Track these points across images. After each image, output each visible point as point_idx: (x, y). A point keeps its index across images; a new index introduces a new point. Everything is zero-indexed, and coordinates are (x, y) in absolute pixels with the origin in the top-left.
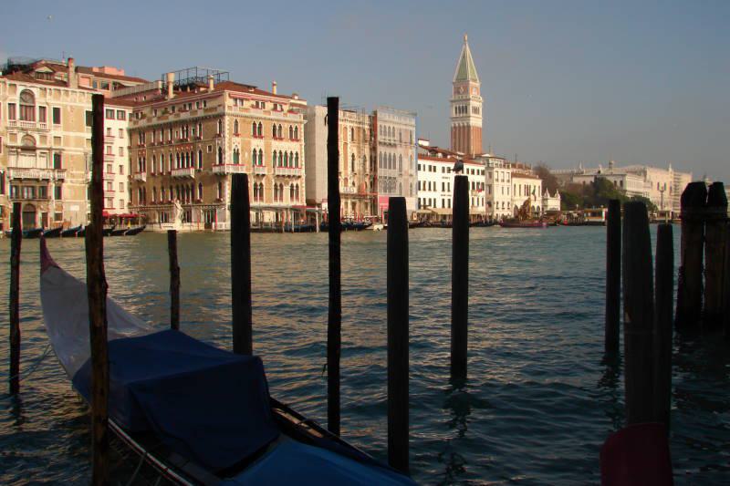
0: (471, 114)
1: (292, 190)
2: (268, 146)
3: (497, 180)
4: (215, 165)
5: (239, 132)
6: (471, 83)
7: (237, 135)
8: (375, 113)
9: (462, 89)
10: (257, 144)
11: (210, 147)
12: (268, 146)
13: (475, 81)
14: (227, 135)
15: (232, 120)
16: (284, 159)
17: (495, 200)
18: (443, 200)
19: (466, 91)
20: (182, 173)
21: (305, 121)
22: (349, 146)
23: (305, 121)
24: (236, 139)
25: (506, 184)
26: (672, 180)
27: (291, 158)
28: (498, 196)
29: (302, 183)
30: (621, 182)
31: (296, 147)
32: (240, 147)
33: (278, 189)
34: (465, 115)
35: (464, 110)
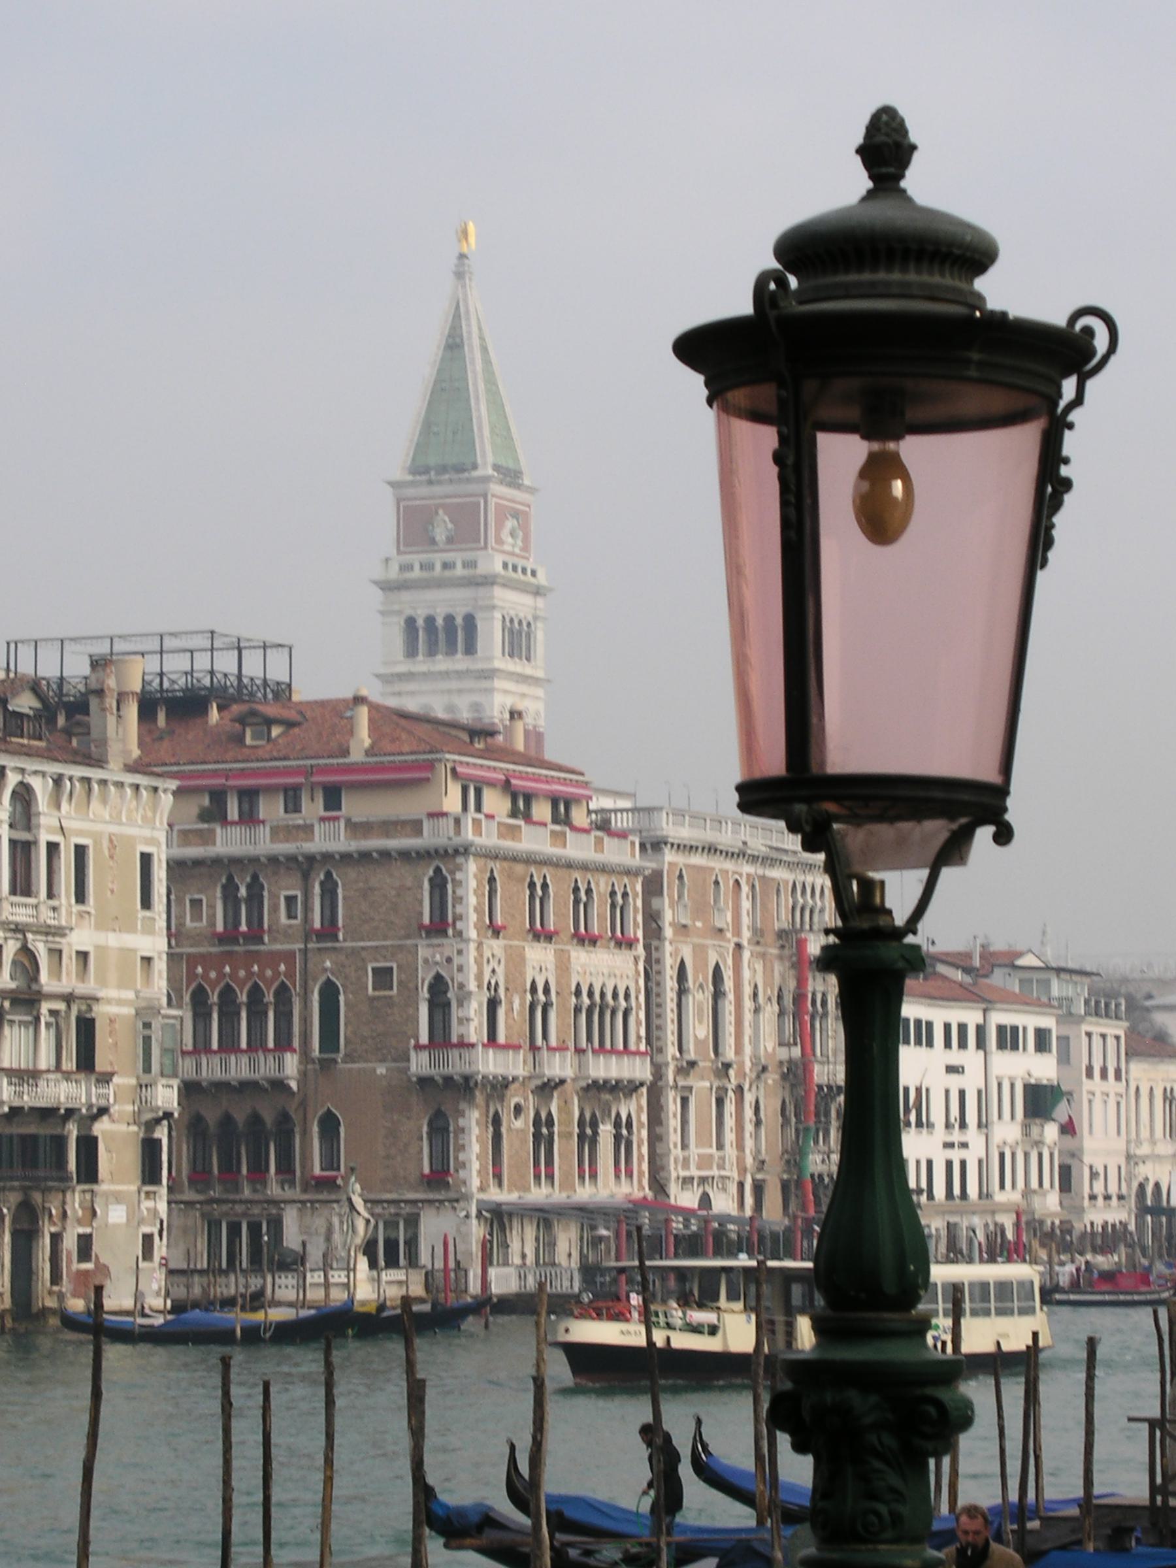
1: (618, 1137)
2: (563, 966)
3: (1090, 1075)
4: (418, 1047)
5: (499, 920)
6: (496, 488)
7: (496, 932)
9: (442, 529)
10: (539, 959)
11: (383, 976)
12: (563, 966)
15: (481, 870)
17: (1087, 1159)
18: (949, 1164)
20: (239, 1068)
22: (746, 955)
24: (496, 946)
27: (613, 1013)
28: (1100, 1146)
29: (640, 1108)
31: (608, 968)
34: (460, 662)
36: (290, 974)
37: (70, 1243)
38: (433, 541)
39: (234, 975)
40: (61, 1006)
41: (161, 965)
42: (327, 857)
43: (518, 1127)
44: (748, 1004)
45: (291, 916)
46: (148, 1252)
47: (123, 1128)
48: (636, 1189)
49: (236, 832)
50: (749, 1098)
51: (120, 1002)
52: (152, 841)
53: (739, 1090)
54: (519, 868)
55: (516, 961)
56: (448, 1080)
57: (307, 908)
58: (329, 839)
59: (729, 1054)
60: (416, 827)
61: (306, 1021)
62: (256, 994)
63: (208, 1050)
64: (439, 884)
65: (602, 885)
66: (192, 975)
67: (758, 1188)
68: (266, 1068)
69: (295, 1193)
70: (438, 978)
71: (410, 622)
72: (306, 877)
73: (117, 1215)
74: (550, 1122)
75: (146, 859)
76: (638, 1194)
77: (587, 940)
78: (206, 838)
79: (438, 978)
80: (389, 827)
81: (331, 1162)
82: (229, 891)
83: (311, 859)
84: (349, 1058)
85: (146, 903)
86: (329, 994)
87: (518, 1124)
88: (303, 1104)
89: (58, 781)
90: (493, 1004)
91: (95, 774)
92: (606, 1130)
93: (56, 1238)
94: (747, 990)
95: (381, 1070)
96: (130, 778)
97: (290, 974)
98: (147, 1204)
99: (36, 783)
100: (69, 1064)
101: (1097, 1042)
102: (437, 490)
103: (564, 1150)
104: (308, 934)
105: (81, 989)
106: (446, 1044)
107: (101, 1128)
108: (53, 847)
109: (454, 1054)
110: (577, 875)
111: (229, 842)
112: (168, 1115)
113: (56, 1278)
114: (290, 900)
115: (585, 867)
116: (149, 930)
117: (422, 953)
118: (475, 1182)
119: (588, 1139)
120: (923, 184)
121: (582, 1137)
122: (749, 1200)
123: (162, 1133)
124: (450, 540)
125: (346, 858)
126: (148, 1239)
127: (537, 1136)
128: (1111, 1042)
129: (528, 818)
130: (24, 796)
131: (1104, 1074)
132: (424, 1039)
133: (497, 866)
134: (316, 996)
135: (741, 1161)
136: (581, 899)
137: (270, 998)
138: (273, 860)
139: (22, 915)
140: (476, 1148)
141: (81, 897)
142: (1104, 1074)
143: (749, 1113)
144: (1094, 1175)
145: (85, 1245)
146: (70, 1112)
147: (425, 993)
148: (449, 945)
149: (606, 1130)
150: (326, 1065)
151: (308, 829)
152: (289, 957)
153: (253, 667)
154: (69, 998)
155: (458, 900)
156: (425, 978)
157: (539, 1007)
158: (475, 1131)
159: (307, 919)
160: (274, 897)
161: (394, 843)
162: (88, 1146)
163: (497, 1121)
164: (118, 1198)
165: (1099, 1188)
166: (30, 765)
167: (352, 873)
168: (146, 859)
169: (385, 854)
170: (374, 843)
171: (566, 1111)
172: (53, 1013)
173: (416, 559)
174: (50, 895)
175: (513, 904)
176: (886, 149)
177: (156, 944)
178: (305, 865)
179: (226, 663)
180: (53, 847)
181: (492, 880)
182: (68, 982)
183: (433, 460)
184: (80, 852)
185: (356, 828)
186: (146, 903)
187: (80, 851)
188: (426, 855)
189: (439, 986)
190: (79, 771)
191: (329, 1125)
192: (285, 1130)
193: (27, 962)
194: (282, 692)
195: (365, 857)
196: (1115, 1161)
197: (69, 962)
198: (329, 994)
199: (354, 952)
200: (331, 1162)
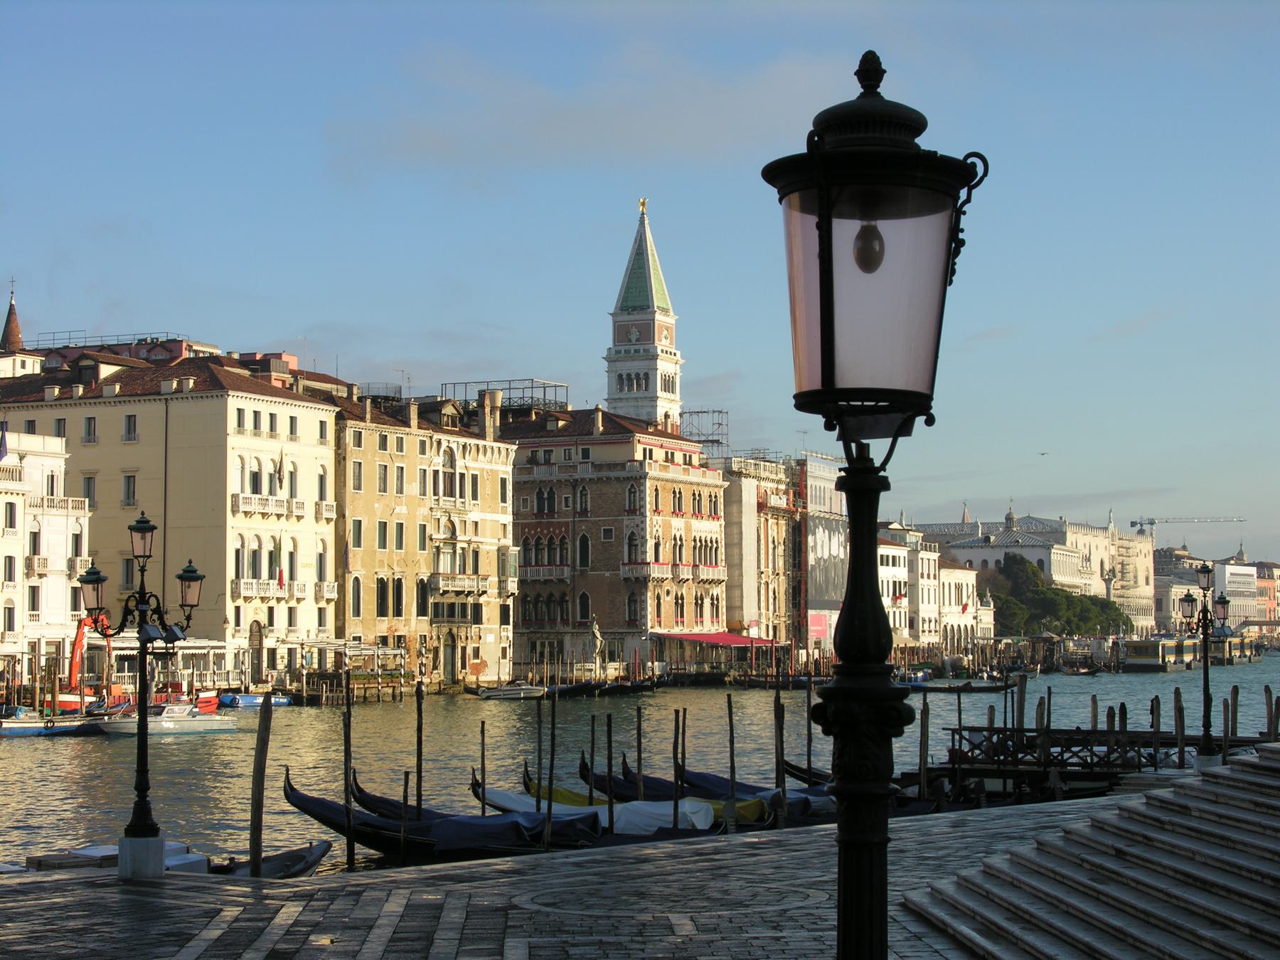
0: (660, 393)
1: (712, 604)
2: (688, 528)
6: (659, 317)
8: (802, 463)
9: (634, 335)
10: (678, 524)
11: (608, 533)
13: (665, 311)
14: (648, 514)
16: (704, 550)
17: (921, 615)
19: (647, 332)
20: (543, 573)
21: (727, 484)
23: (727, 484)
25: (932, 582)
26: (1113, 551)
28: (927, 610)
30: (1041, 562)
31: (710, 529)
32: (660, 533)
33: (699, 604)
34: (642, 394)
35: (645, 379)
36: (567, 531)
37: (469, 651)
38: (630, 340)
39: (542, 532)
40: (465, 545)
41: (510, 528)
42: (583, 480)
43: (668, 601)
44: (771, 546)
45: (567, 506)
46: (504, 656)
47: (492, 600)
48: (722, 628)
49: (543, 468)
50: (771, 587)
51: (491, 544)
52: (507, 473)
53: (767, 584)
54: (669, 485)
55: (667, 526)
56: (637, 579)
57: (575, 502)
59: (763, 568)
60: (623, 466)
62: (551, 541)
63: (530, 565)
65: (705, 493)
66: (523, 532)
67: (775, 628)
68: (555, 574)
69: (569, 629)
71: (620, 376)
72: (574, 488)
73: (490, 638)
74: (682, 598)
75: (503, 481)
76: (721, 630)
78: (530, 471)
79: (633, 533)
80: (612, 466)
82: (540, 494)
84: (593, 569)
85: (504, 500)
86: (584, 541)
87: (668, 599)
88: (573, 589)
89: (464, 447)
90: (657, 546)
91: (481, 443)
92: (707, 602)
93: (464, 649)
94: (770, 540)
95: (607, 574)
96: (496, 445)
97: (567, 531)
98: (504, 634)
99: (454, 446)
100: (469, 570)
101: (926, 562)
102: (632, 317)
103: (689, 608)
104: (575, 513)
105: (474, 539)
106: (636, 563)
107: (482, 600)
108: (462, 476)
110: (695, 487)
111: (539, 473)
112: (513, 594)
113: (464, 666)
114: (566, 499)
115: (698, 484)
116: (504, 511)
117: (626, 522)
118: (649, 625)
119: (699, 604)
120: (889, 90)
121: (696, 604)
122: (771, 633)
123: (510, 602)
124: (638, 340)
126: (504, 650)
127: (677, 603)
128: (932, 563)
129: (672, 461)
130: (450, 454)
131: (929, 577)
132: (626, 561)
133: (659, 484)
134: (578, 543)
135: (767, 616)
136: (697, 498)
137: (557, 542)
138: (559, 481)
139: (449, 506)
140: (649, 609)
141: (475, 497)
142: (929, 577)
143: (771, 594)
144: (924, 620)
145: (476, 652)
146: (470, 593)
147: (626, 541)
148: (637, 519)
149: (707, 602)
152: (567, 523)
153: (550, 396)
157: (678, 546)
158: (649, 601)
159: (574, 508)
160: (560, 497)
161: (613, 474)
162: (477, 608)
163: (659, 598)
164: (491, 631)
165: (926, 626)
166: (452, 438)
168: (503, 481)
170: (604, 474)
171: (689, 592)
172: (463, 549)
173: (623, 349)
174: (461, 497)
175: (667, 502)
176: (870, 70)
177: (508, 519)
178: (575, 484)
179: (538, 394)
180: (462, 476)
181: (656, 490)
182: (470, 535)
183: (630, 304)
184: (475, 478)
186: (504, 500)
187: (475, 478)
188: (628, 479)
189: (632, 538)
190: (473, 441)
192: (562, 601)
194: (563, 406)
196: (934, 615)
197: (470, 527)
198: (584, 541)
200: (585, 614)
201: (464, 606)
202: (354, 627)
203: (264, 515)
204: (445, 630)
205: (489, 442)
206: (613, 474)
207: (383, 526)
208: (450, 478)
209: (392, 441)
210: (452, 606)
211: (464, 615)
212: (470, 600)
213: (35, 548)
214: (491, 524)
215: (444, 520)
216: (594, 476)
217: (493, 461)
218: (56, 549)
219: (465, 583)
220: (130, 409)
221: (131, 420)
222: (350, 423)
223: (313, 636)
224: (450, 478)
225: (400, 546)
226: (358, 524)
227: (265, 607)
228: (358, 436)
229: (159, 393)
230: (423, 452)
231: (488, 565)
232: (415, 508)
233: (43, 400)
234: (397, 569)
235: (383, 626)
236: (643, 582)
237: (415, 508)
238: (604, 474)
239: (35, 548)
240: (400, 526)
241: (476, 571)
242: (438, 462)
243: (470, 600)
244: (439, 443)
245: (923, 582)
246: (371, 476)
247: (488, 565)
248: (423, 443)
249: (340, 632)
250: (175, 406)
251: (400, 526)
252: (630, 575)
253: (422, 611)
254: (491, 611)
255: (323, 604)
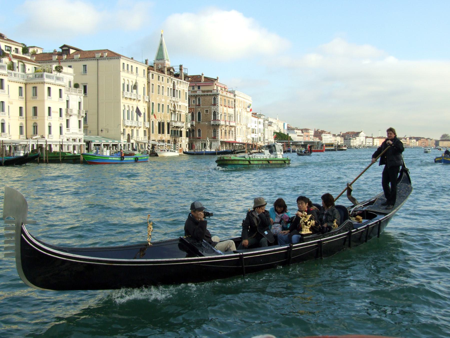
11: (207, 111)
36: (194, 111)
42: (199, 95)
43: (223, 131)
55: (223, 109)
57: (196, 102)
58: (199, 93)
60: (211, 91)
61: (196, 117)
64: (215, 99)
70: (215, 111)
72: (196, 98)
73: (183, 141)
77: (229, 107)
79: (215, 111)
80: (208, 91)
81: (200, 135)
83: (197, 95)
88: (196, 128)
95: (207, 123)
97: (194, 111)
99: (175, 81)
104: (196, 106)
109: (217, 121)
125: (202, 95)
148: (216, 107)
149: (231, 132)
150: (199, 123)
151: (196, 92)
152: (194, 109)
154: (179, 111)
155: (217, 101)
156: (213, 111)
161: (209, 93)
162: (181, 132)
166: (175, 79)
167: (202, 97)
169: (207, 95)
170: (206, 93)
185: (203, 91)
188: (213, 95)
189: (215, 113)
191: (199, 131)
193: (175, 107)
195: (204, 95)
197: (179, 106)
199: (203, 108)
200: (200, 135)
201: (178, 131)
202: (152, 138)
203: (130, 99)
204: (174, 139)
205: (183, 81)
206: (209, 93)
207: (159, 104)
208: (174, 90)
209: (161, 77)
210: (175, 131)
211: (178, 134)
212: (179, 130)
213: (68, 107)
214: (183, 105)
215: (173, 104)
216: (203, 94)
217: (184, 87)
218: (74, 106)
219: (179, 124)
220: (85, 63)
221: (85, 66)
222: (151, 71)
223: (143, 139)
224: (174, 90)
225: (163, 112)
226: (153, 103)
227: (131, 129)
228: (153, 75)
229: (95, 57)
230: (168, 82)
231: (183, 119)
232: (166, 99)
233: (52, 60)
234: (162, 119)
235: (160, 136)
236: (218, 126)
237: (166, 99)
238: (206, 93)
239: (68, 107)
240: (163, 105)
241: (180, 121)
242: (172, 85)
243: (179, 130)
244: (172, 79)
245: (266, 129)
246: (156, 88)
247: (183, 119)
248: (168, 79)
249: (149, 138)
250: (101, 62)
251: (163, 105)
252: (213, 124)
253: (168, 133)
254: (184, 134)
255: (145, 129)
